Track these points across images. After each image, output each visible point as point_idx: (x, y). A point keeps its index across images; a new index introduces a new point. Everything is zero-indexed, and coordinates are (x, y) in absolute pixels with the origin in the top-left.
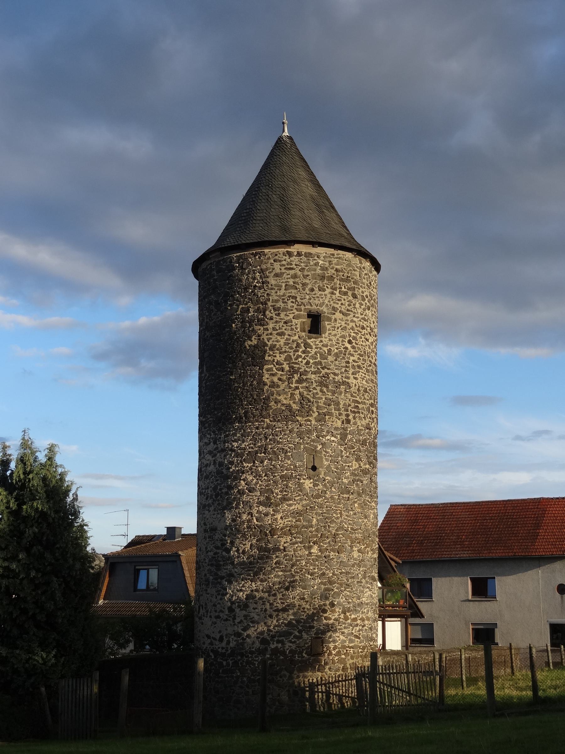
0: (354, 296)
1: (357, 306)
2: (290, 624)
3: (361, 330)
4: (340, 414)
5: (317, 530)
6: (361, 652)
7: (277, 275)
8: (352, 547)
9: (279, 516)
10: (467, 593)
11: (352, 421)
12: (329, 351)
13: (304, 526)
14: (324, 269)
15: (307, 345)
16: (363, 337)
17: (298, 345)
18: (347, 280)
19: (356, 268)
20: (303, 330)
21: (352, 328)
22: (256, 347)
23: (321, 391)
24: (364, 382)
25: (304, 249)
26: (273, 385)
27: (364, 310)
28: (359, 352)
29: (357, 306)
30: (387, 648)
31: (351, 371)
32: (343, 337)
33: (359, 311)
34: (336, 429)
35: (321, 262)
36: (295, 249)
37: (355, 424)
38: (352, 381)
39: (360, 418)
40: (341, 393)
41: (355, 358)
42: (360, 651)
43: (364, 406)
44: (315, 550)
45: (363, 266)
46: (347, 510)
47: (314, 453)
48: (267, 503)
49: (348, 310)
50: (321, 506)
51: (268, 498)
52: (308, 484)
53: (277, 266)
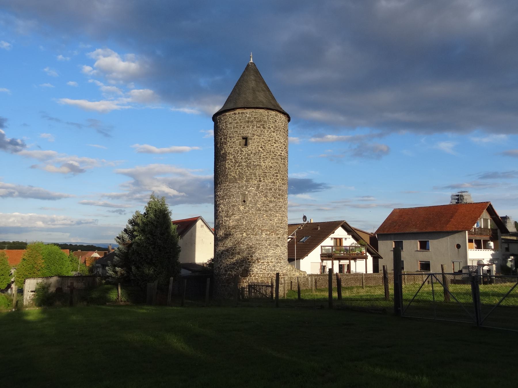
0: (264, 128)
1: (266, 132)
2: (234, 264)
4: (256, 178)
5: (245, 227)
7: (230, 123)
9: (231, 221)
10: (417, 247)
11: (263, 181)
12: (251, 152)
13: (240, 225)
14: (249, 118)
15: (242, 151)
17: (238, 151)
18: (260, 121)
20: (240, 145)
21: (263, 142)
22: (224, 153)
23: (248, 169)
24: (270, 164)
25: (240, 111)
26: (229, 169)
27: (270, 133)
29: (266, 132)
30: (319, 273)
31: (262, 160)
32: (258, 146)
34: (255, 185)
35: (248, 115)
36: (237, 111)
38: (262, 164)
39: (267, 179)
40: (257, 169)
41: (265, 154)
44: (244, 235)
46: (260, 218)
47: (244, 195)
48: (227, 216)
50: (247, 217)
51: (227, 214)
52: (242, 208)
53: (230, 119)
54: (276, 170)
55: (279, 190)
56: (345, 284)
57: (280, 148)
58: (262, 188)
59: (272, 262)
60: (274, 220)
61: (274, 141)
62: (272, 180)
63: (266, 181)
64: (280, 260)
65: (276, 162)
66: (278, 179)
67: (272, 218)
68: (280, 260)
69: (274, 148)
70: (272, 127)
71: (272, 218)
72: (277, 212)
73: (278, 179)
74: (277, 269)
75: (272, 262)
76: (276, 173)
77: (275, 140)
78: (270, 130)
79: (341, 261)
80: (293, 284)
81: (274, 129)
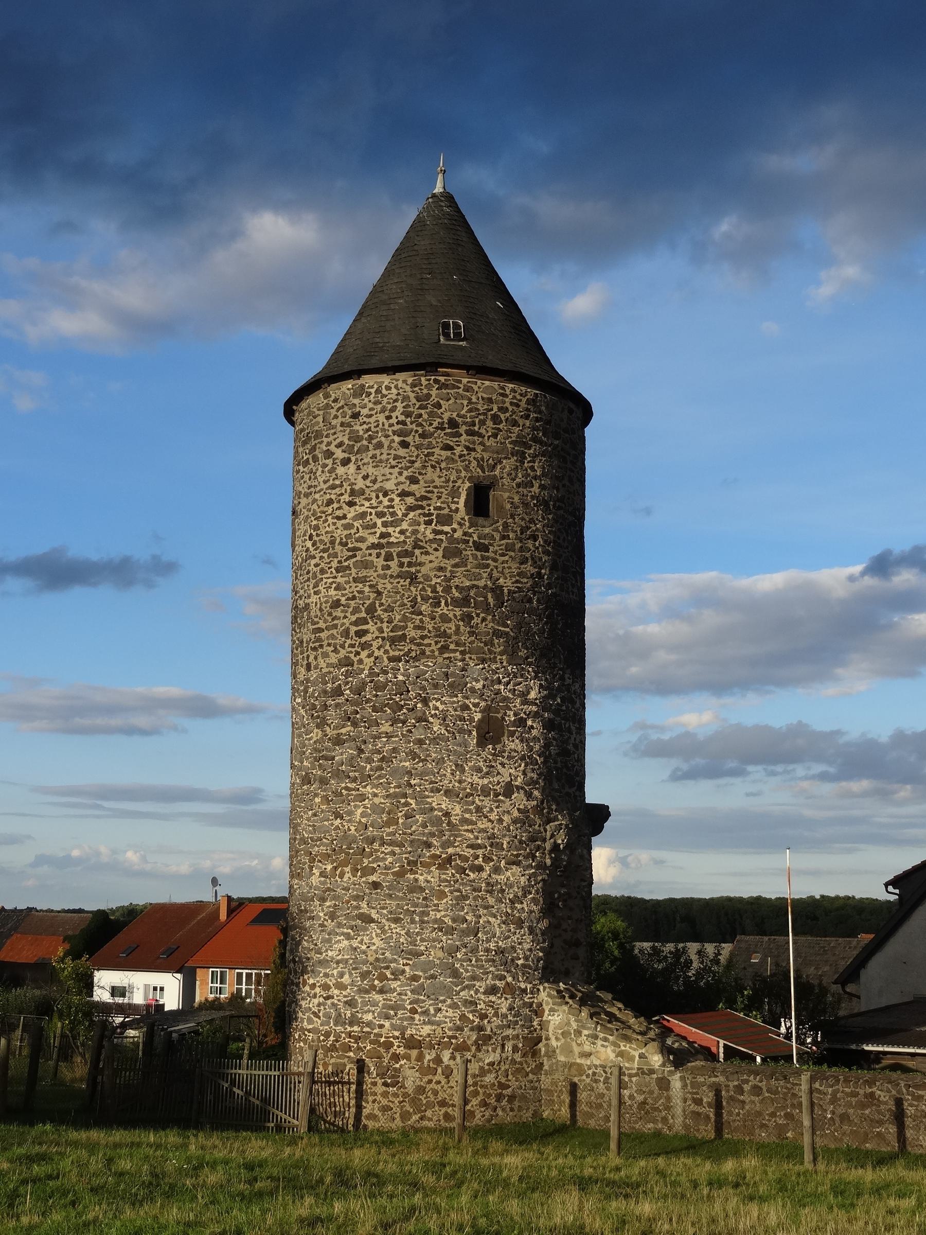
0: (315, 459)
3: (326, 509)
6: (324, 1041)
8: (311, 868)
11: (314, 663)
16: (329, 518)
19: (317, 412)
24: (332, 592)
28: (322, 547)
33: (321, 480)
39: (325, 655)
41: (317, 560)
42: (322, 1038)
43: (334, 632)
45: (332, 399)
49: (310, 487)
54: (356, 610)
55: (379, 687)
57: (380, 515)
58: (312, 696)
59: (341, 987)
60: (350, 813)
62: (343, 653)
63: (322, 664)
65: (355, 580)
66: (365, 646)
69: (348, 527)
71: (343, 809)
73: (364, 646)
74: (369, 1017)
75: (341, 987)
76: (356, 623)
77: (353, 493)
78: (329, 462)
80: (582, 1096)
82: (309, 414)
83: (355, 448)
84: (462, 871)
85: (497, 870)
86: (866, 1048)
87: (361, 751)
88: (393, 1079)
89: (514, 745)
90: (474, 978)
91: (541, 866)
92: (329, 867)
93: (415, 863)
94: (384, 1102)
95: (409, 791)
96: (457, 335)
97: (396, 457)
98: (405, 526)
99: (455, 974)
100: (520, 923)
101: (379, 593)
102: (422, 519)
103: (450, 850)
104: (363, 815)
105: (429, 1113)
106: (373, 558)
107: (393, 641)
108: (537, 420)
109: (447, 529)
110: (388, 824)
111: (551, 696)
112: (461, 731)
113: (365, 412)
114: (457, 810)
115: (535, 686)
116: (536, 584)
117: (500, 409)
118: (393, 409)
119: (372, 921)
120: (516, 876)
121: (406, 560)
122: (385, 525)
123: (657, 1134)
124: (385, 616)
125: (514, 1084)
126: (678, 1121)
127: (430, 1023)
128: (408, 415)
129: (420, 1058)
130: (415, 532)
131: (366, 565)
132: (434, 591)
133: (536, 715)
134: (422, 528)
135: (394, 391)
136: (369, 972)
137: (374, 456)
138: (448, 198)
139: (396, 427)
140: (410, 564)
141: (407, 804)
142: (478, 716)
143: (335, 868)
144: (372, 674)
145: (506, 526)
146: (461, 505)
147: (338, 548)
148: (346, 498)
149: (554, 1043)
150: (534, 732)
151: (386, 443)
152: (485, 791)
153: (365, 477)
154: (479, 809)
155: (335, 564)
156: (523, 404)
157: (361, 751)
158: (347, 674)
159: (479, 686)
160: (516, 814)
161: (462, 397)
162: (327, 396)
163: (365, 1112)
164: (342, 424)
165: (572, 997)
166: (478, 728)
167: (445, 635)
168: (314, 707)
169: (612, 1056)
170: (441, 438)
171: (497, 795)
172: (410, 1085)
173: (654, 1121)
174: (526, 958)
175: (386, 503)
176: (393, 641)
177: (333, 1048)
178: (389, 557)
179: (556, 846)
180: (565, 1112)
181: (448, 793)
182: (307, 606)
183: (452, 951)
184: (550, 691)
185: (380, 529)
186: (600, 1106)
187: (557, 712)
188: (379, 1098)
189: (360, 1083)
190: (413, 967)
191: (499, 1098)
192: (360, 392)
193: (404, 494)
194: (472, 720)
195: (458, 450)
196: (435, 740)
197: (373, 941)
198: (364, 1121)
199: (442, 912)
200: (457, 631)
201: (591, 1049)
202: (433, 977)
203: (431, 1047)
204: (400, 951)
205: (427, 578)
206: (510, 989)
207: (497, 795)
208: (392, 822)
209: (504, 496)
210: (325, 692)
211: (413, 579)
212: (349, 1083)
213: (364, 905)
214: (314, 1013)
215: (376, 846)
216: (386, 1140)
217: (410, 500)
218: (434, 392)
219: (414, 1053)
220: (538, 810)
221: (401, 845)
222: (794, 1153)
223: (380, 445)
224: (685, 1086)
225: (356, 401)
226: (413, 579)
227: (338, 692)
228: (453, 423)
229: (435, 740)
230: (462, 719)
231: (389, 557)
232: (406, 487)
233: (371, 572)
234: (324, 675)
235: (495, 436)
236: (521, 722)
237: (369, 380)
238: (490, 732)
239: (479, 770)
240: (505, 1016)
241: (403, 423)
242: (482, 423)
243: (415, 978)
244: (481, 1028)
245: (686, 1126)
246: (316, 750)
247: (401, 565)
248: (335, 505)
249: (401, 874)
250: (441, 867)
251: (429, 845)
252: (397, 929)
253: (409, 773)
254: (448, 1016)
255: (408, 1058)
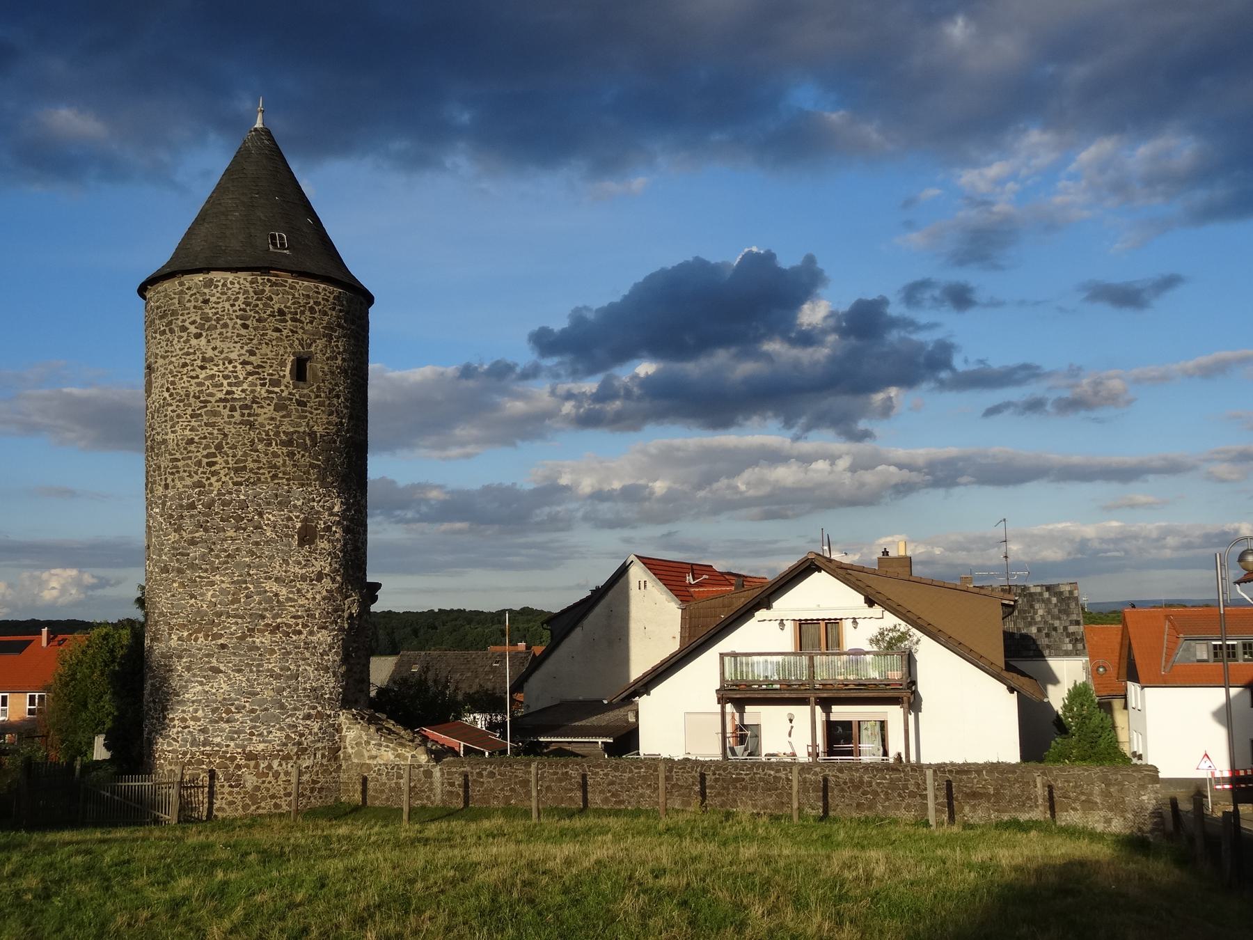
0: (172, 331)
24: (187, 432)
37: (174, 487)
39: (181, 479)
41: (174, 408)
56: (606, 800)
60: (202, 595)
61: (199, 363)
62: (196, 478)
63: (179, 485)
64: (228, 712)
65: (206, 424)
66: (214, 473)
67: (197, 591)
68: (228, 712)
69: (199, 384)
70: (193, 323)
71: (197, 591)
72: (215, 570)
74: (218, 740)
76: (207, 456)
77: (204, 359)
78: (184, 334)
79: (835, 708)
80: (371, 785)
81: (201, 327)
82: (165, 296)
83: (205, 326)
84: (287, 634)
85: (311, 633)
86: (542, 739)
87: (212, 550)
88: (238, 783)
89: (323, 544)
90: (295, 709)
91: (341, 629)
92: (186, 634)
93: (253, 630)
94: (230, 798)
95: (248, 579)
96: (282, 245)
97: (238, 335)
98: (245, 386)
99: (282, 707)
100: (327, 669)
101: (225, 435)
102: (258, 382)
103: (279, 620)
104: (213, 596)
105: (263, 804)
106: (220, 409)
107: (236, 470)
108: (340, 311)
109: (277, 390)
110: (232, 602)
111: (348, 509)
112: (287, 536)
113: (213, 299)
114: (284, 591)
115: (338, 501)
116: (339, 430)
117: (315, 303)
118: (236, 299)
119: (221, 672)
120: (324, 637)
121: (246, 412)
122: (230, 385)
123: (423, 807)
124: (230, 452)
125: (322, 780)
126: (438, 798)
127: (264, 741)
128: (248, 304)
129: (257, 766)
130: (253, 391)
131: (215, 414)
132: (267, 435)
133: (339, 523)
134: (258, 388)
135: (237, 286)
136: (218, 708)
137: (221, 334)
138: (266, 132)
139: (239, 313)
140: (249, 415)
141: (247, 588)
142: (298, 525)
143: (191, 635)
144: (219, 494)
145: (319, 388)
146: (287, 373)
147: (192, 400)
148: (199, 363)
149: (350, 750)
150: (337, 535)
151: (231, 325)
152: (304, 578)
153: (214, 349)
154: (299, 591)
155: (189, 411)
156: (331, 299)
157: (212, 550)
158: (200, 494)
159: (299, 503)
160: (325, 593)
161: (288, 293)
162: (181, 284)
163: (215, 806)
164: (195, 307)
165: (362, 718)
166: (299, 533)
167: (275, 467)
168: (171, 516)
169: (392, 757)
170: (273, 322)
171: (312, 580)
172: (249, 786)
173: (421, 799)
174: (331, 693)
175: (231, 369)
176: (236, 470)
177: (190, 763)
178: (233, 409)
179: (351, 614)
180: (358, 797)
181: (277, 580)
182: (164, 442)
183: (279, 691)
184: (347, 506)
185: (226, 388)
186: (383, 791)
187: (351, 520)
188: (226, 796)
189: (211, 786)
190: (252, 703)
191: (312, 790)
192: (208, 284)
193: (244, 363)
194: (294, 527)
195: (285, 332)
196: (267, 542)
197: (221, 686)
198: (215, 813)
199: (272, 663)
200: (284, 464)
201: (374, 752)
202: (266, 709)
203: (265, 758)
204: (240, 692)
205: (262, 425)
206: (320, 715)
207: (312, 580)
208: (237, 601)
209: (317, 367)
210: (181, 506)
211: (252, 425)
212: (203, 787)
213: (214, 660)
214: (174, 739)
215: (223, 618)
216: (228, 825)
217: (249, 368)
218: (267, 289)
219: (252, 763)
220: (339, 590)
221: (242, 617)
222: (527, 814)
223: (225, 326)
224: (443, 774)
225: (206, 291)
226: (252, 425)
227: (192, 506)
228: (281, 312)
229: (267, 542)
230: (288, 527)
231: (233, 409)
232: (247, 358)
233: (219, 419)
234: (180, 494)
235: (311, 322)
236: (328, 529)
237: (216, 275)
238: (307, 536)
239: (299, 563)
240: (316, 734)
241: (244, 310)
242: (303, 313)
243: (253, 711)
244: (300, 743)
245: (443, 801)
246: (174, 548)
247: (243, 415)
248: (190, 368)
249: (243, 638)
250: (272, 632)
251: (263, 617)
252: (239, 676)
253: (249, 566)
254: (277, 736)
255: (247, 766)
